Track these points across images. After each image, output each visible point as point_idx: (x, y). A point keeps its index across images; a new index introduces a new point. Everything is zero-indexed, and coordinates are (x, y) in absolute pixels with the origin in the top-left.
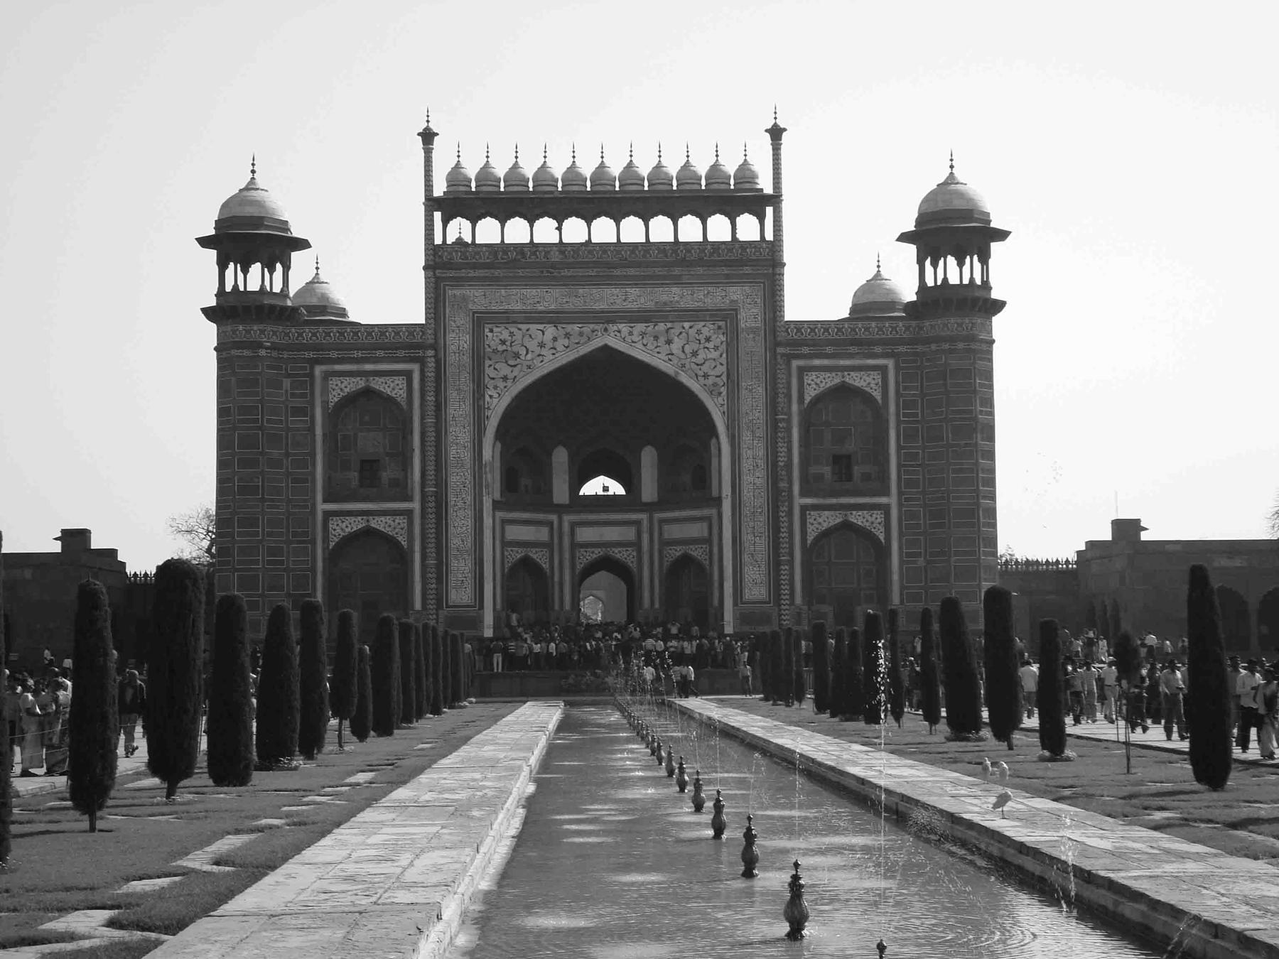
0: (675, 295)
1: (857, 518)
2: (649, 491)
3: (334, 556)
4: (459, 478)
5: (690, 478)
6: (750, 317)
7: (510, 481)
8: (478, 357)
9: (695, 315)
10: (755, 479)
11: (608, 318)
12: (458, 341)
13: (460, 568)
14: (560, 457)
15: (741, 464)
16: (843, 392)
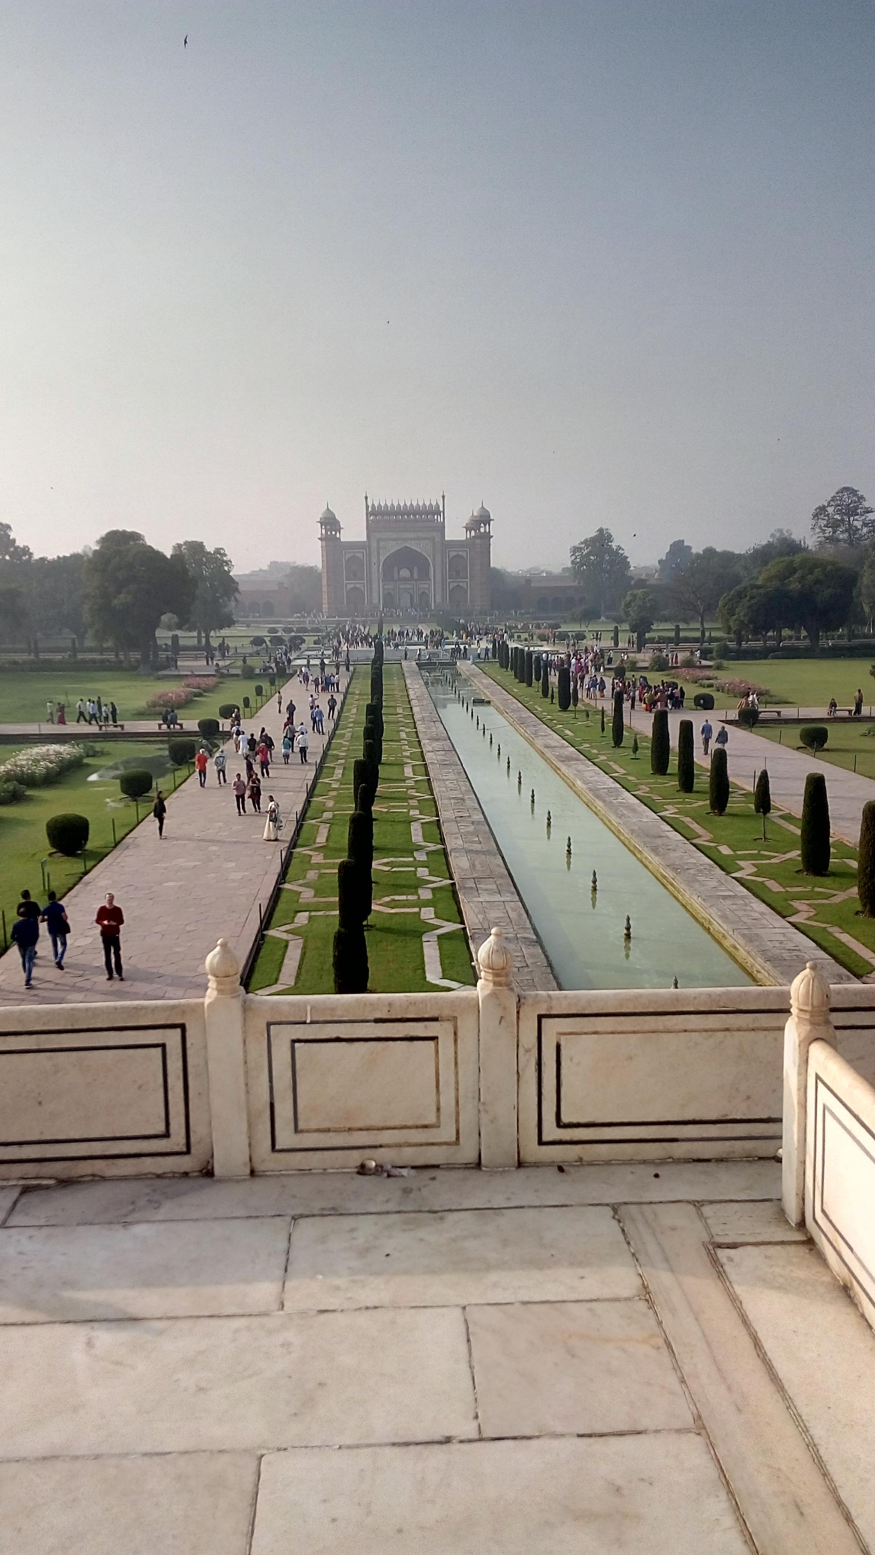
0: (420, 534)
1: (461, 584)
2: (416, 576)
3: (348, 593)
4: (375, 576)
5: (424, 573)
6: (438, 539)
7: (384, 575)
8: (378, 548)
9: (425, 539)
10: (439, 576)
11: (406, 540)
12: (374, 545)
13: (375, 595)
14: (396, 569)
15: (435, 572)
16: (458, 556)
